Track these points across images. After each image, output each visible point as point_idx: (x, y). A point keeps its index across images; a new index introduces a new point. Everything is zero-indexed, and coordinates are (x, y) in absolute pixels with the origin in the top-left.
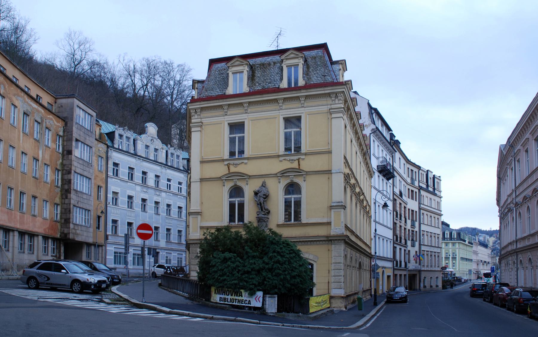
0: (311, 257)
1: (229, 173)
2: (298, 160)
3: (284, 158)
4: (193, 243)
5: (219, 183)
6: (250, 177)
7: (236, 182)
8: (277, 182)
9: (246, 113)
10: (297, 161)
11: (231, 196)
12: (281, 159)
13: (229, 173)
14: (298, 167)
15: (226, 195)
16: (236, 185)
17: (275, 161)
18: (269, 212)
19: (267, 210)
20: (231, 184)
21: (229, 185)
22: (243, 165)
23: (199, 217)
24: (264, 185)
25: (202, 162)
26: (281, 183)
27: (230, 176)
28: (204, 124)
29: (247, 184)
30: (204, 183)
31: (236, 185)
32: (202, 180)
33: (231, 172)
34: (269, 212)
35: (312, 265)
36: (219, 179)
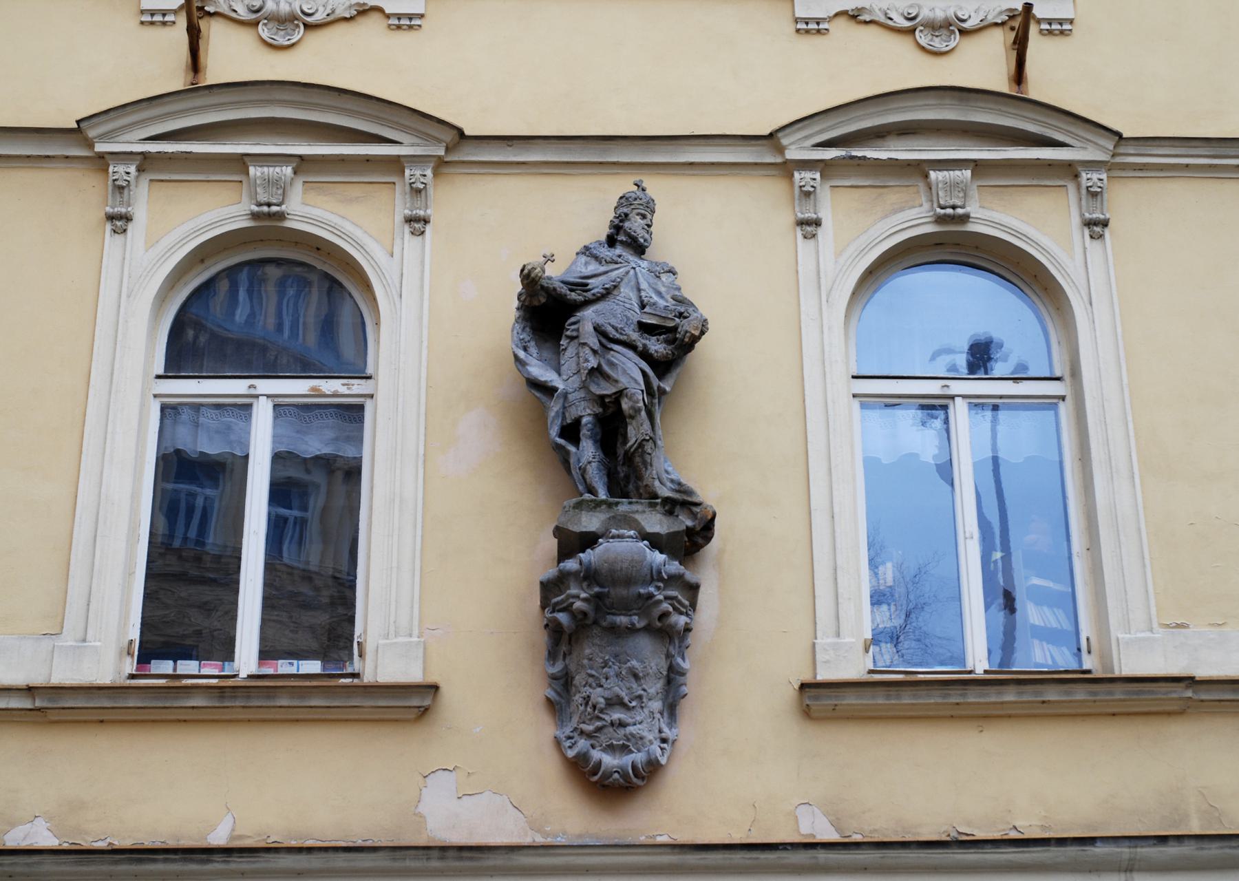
1: (197, 89)
5: (72, 197)
6: (455, 147)
7: (283, 189)
8: (784, 218)
11: (189, 346)
13: (196, 90)
14: (999, 82)
15: (141, 339)
16: (268, 222)
20: (218, 211)
21: (185, 220)
24: (625, 237)
26: (826, 233)
27: (193, 128)
29: (417, 223)
31: (268, 222)
33: (214, 73)
34: (693, 535)
36: (73, 144)
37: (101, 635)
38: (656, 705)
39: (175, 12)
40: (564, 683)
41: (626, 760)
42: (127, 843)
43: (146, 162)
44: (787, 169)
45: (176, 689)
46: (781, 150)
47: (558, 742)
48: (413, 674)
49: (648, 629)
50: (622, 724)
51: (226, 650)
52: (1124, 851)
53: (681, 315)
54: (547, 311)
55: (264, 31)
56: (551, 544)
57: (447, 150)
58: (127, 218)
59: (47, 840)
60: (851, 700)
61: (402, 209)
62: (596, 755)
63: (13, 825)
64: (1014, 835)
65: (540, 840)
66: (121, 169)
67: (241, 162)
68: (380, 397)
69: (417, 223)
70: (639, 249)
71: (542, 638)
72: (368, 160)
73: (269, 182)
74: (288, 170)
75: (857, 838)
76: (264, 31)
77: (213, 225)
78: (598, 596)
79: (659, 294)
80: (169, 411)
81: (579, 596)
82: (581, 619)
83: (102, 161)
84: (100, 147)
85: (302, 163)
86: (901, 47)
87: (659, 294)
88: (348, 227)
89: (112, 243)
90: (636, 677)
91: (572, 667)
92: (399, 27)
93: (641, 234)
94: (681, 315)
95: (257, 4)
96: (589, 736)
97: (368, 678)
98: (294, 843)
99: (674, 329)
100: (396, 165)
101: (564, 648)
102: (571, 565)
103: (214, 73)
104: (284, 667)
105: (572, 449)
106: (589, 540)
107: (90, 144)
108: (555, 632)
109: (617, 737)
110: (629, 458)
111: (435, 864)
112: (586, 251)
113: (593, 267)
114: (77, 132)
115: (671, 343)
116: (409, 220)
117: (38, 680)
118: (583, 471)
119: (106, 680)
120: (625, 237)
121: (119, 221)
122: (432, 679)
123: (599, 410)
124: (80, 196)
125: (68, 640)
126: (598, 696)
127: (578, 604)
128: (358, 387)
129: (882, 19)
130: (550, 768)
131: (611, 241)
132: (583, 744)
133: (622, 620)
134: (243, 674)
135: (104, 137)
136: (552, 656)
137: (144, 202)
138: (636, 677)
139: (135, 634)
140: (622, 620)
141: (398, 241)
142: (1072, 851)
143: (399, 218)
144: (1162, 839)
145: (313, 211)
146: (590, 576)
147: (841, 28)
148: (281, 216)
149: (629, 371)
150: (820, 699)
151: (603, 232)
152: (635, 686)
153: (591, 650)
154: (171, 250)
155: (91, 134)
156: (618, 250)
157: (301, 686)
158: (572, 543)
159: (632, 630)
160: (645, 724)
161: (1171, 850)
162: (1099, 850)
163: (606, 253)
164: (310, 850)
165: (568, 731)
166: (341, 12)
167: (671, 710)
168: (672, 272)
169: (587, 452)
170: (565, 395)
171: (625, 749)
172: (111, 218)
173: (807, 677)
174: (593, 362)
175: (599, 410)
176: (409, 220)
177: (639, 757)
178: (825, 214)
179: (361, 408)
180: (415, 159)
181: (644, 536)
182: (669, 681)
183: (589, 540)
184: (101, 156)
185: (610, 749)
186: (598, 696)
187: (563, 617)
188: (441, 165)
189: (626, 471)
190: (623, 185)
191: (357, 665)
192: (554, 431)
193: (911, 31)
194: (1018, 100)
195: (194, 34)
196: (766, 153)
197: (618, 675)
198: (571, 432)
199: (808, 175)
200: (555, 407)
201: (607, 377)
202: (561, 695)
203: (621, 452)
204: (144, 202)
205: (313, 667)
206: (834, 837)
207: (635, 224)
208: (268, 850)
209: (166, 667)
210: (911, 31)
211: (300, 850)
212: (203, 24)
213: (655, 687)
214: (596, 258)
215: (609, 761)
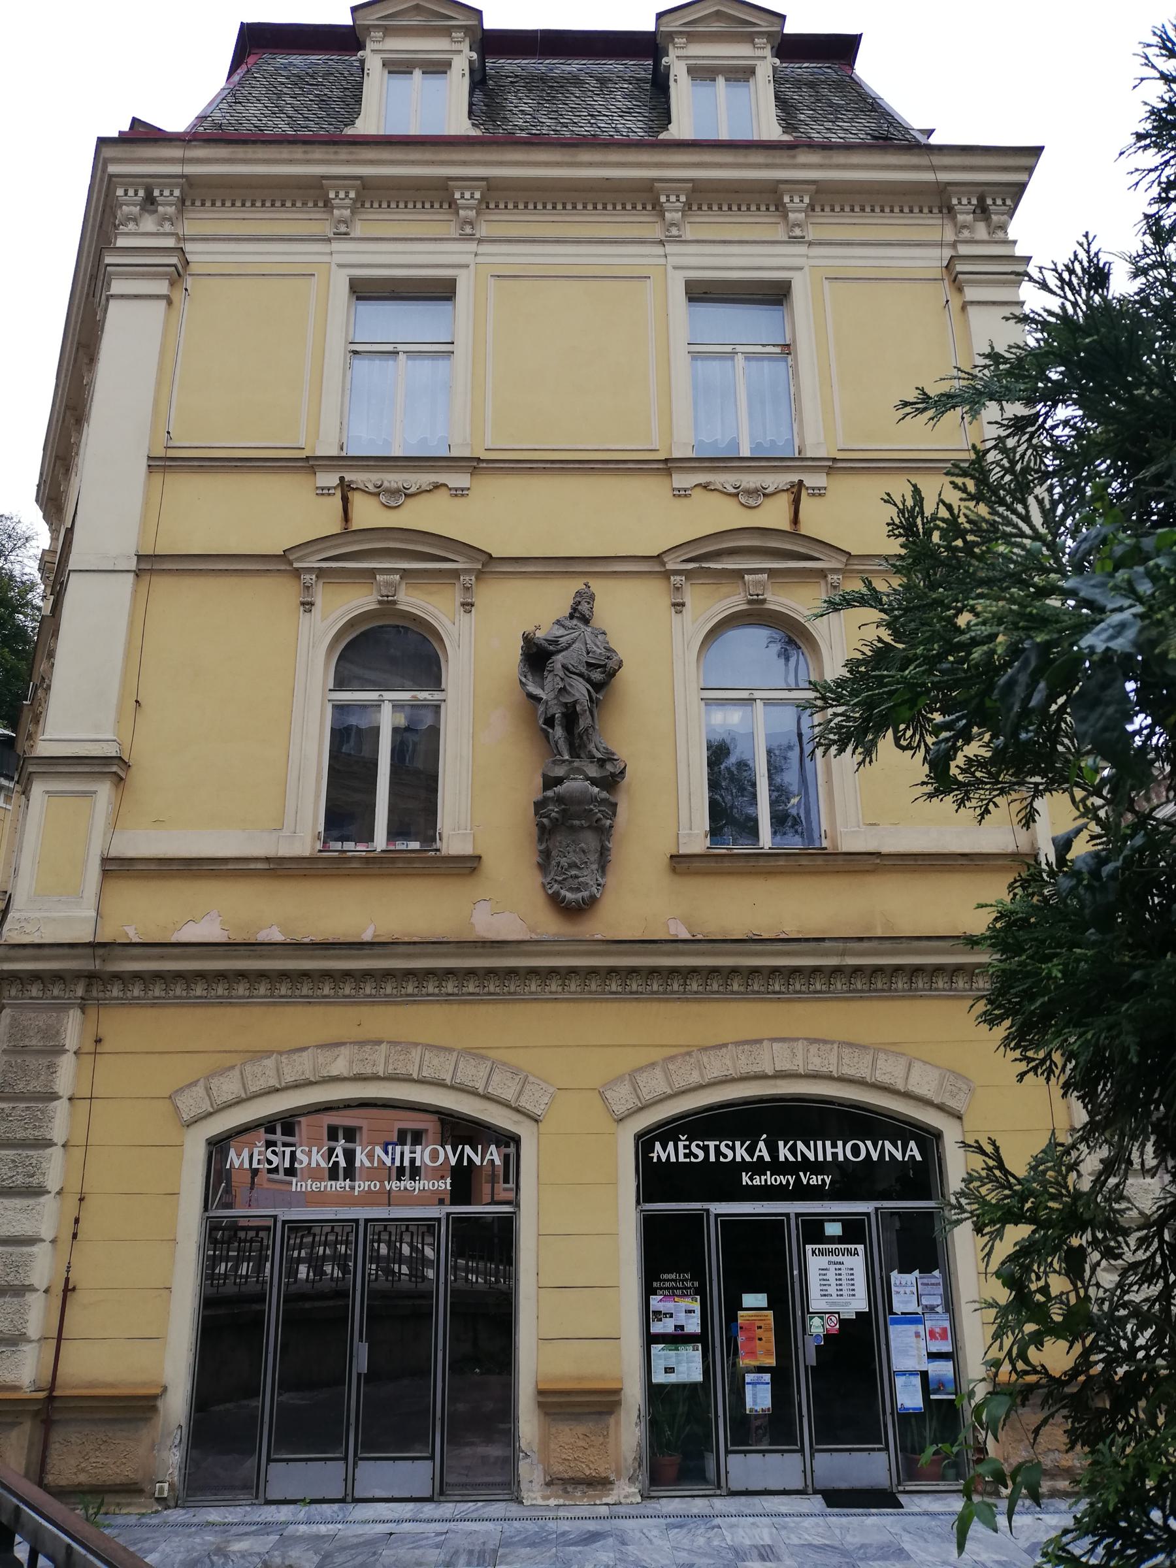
0: (923, 1082)
2: (796, 491)
3: (702, 478)
4: (36, 977)
5: (280, 593)
6: (488, 565)
7: (395, 587)
8: (665, 602)
9: (469, 238)
10: (784, 501)
12: (682, 480)
13: (347, 533)
14: (785, 525)
16: (388, 605)
17: (649, 492)
18: (623, 772)
19: (608, 758)
20: (356, 601)
22: (442, 496)
23: (104, 790)
24: (580, 614)
25: (163, 464)
27: (344, 554)
28: (193, 268)
29: (468, 606)
30: (163, 586)
31: (388, 605)
32: (150, 566)
33: (357, 523)
35: (929, 1139)
36: (281, 563)
37: (303, 829)
38: (595, 867)
39: (335, 488)
40: (546, 855)
41: (579, 895)
42: (318, 938)
43: (321, 573)
44: (667, 574)
45: (344, 858)
46: (663, 564)
47: (543, 886)
48: (466, 849)
49: (589, 827)
50: (577, 877)
51: (370, 838)
52: (841, 945)
53: (608, 658)
54: (536, 656)
55: (383, 499)
56: (539, 781)
57: (483, 565)
58: (312, 604)
59: (278, 937)
60: (697, 864)
61: (459, 600)
62: (563, 892)
63: (262, 929)
64: (783, 936)
65: (535, 937)
66: (308, 577)
67: (372, 573)
68: (449, 701)
69: (468, 606)
70: (586, 621)
71: (535, 831)
72: (440, 571)
73: (388, 584)
74: (397, 577)
75: (700, 937)
76: (383, 499)
77: (358, 607)
78: (564, 810)
79: (596, 645)
80: (340, 709)
81: (554, 810)
82: (554, 822)
83: (297, 573)
84: (296, 565)
85: (405, 573)
86: (730, 505)
87: (596, 645)
88: (431, 609)
89: (304, 618)
90: (584, 852)
91: (551, 847)
92: (456, 495)
93: (587, 613)
94: (608, 658)
95: (379, 483)
96: (559, 882)
97: (444, 852)
98: (406, 939)
99: (605, 666)
100: (456, 574)
101: (546, 836)
102: (550, 793)
103: (357, 523)
104: (400, 845)
105: (550, 731)
106: (559, 781)
107: (292, 564)
108: (541, 827)
109: (574, 884)
110: (581, 737)
111: (480, 950)
112: (558, 622)
113: (562, 632)
114: (284, 557)
115: (603, 674)
116: (463, 605)
117: (270, 852)
118: (556, 743)
119: (307, 853)
120: (580, 614)
121: (308, 606)
122: (478, 853)
123: (564, 710)
124: (285, 592)
125: (286, 832)
126: (564, 862)
127: (553, 814)
128: (437, 696)
129: (721, 488)
130: (540, 900)
131: (571, 617)
132: (556, 886)
133: (576, 822)
134: (379, 850)
135: (299, 559)
136: (540, 840)
137: (320, 596)
138: (584, 852)
139: (321, 828)
140: (576, 822)
141: (457, 617)
142: (813, 945)
143: (458, 604)
144: (861, 939)
145: (412, 600)
146: (560, 800)
147: (698, 494)
148: (395, 602)
149: (580, 690)
150: (680, 863)
151: (567, 611)
152: (583, 856)
153: (560, 838)
154: (335, 622)
155: (291, 558)
156: (575, 622)
157: (409, 858)
158: (550, 782)
159: (582, 828)
160: (588, 876)
161: (865, 945)
162: (827, 944)
163: (568, 623)
164: (415, 943)
165: (549, 879)
166: (424, 487)
167: (603, 868)
168: (604, 633)
169: (559, 732)
170: (547, 702)
171: (578, 890)
172: (303, 604)
173: (674, 852)
174: (561, 685)
175: (564, 710)
176: (463, 605)
177: (586, 894)
178: (688, 600)
179: (438, 707)
180: (467, 571)
181: (587, 778)
182: (601, 854)
183: (559, 781)
184: (297, 569)
185: (571, 890)
186: (564, 862)
187: (545, 820)
188: (480, 575)
189: (578, 743)
190: (577, 585)
191: (438, 844)
192: (541, 721)
193: (737, 495)
194: (794, 535)
195: (345, 501)
196: (655, 566)
197: (574, 851)
198: (550, 721)
199: (678, 578)
200: (541, 708)
201: (569, 693)
202: (545, 862)
203: (577, 732)
204: (320, 596)
205: (415, 845)
206: (688, 936)
207: (584, 607)
208: (393, 943)
209: (337, 845)
210: (737, 495)
211: (409, 943)
212: (349, 494)
213: (594, 857)
214: (563, 626)
215: (570, 895)
